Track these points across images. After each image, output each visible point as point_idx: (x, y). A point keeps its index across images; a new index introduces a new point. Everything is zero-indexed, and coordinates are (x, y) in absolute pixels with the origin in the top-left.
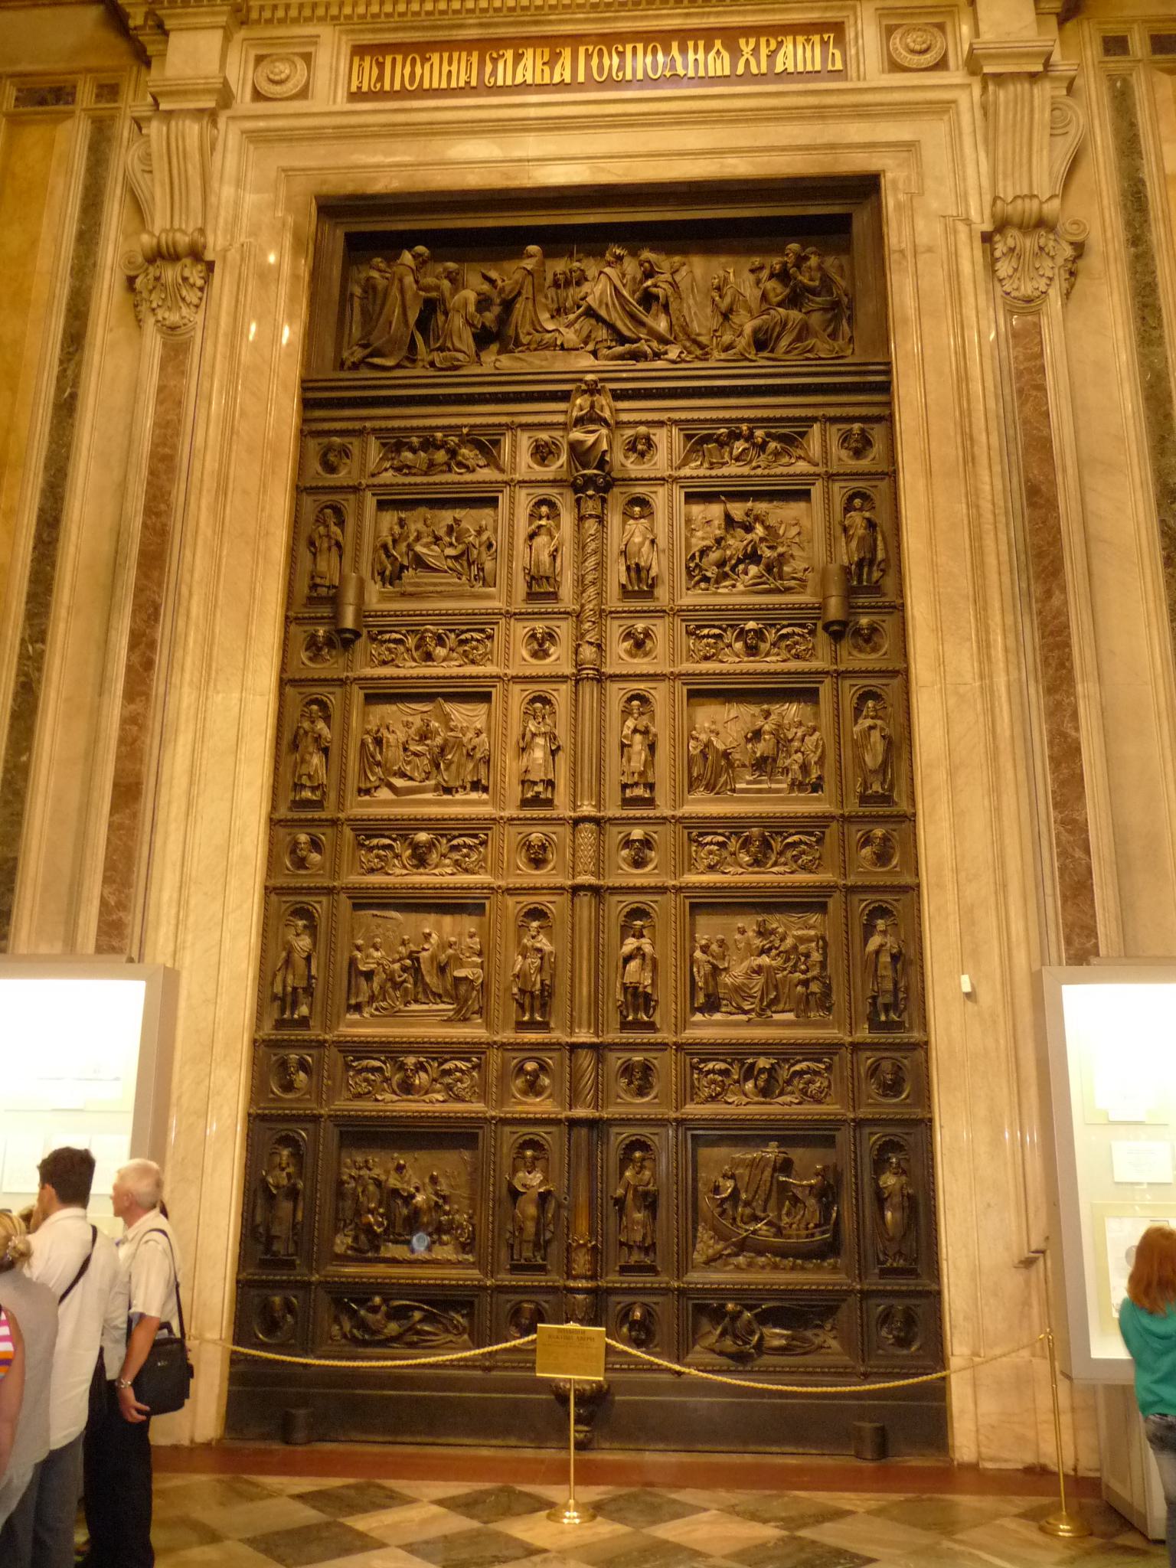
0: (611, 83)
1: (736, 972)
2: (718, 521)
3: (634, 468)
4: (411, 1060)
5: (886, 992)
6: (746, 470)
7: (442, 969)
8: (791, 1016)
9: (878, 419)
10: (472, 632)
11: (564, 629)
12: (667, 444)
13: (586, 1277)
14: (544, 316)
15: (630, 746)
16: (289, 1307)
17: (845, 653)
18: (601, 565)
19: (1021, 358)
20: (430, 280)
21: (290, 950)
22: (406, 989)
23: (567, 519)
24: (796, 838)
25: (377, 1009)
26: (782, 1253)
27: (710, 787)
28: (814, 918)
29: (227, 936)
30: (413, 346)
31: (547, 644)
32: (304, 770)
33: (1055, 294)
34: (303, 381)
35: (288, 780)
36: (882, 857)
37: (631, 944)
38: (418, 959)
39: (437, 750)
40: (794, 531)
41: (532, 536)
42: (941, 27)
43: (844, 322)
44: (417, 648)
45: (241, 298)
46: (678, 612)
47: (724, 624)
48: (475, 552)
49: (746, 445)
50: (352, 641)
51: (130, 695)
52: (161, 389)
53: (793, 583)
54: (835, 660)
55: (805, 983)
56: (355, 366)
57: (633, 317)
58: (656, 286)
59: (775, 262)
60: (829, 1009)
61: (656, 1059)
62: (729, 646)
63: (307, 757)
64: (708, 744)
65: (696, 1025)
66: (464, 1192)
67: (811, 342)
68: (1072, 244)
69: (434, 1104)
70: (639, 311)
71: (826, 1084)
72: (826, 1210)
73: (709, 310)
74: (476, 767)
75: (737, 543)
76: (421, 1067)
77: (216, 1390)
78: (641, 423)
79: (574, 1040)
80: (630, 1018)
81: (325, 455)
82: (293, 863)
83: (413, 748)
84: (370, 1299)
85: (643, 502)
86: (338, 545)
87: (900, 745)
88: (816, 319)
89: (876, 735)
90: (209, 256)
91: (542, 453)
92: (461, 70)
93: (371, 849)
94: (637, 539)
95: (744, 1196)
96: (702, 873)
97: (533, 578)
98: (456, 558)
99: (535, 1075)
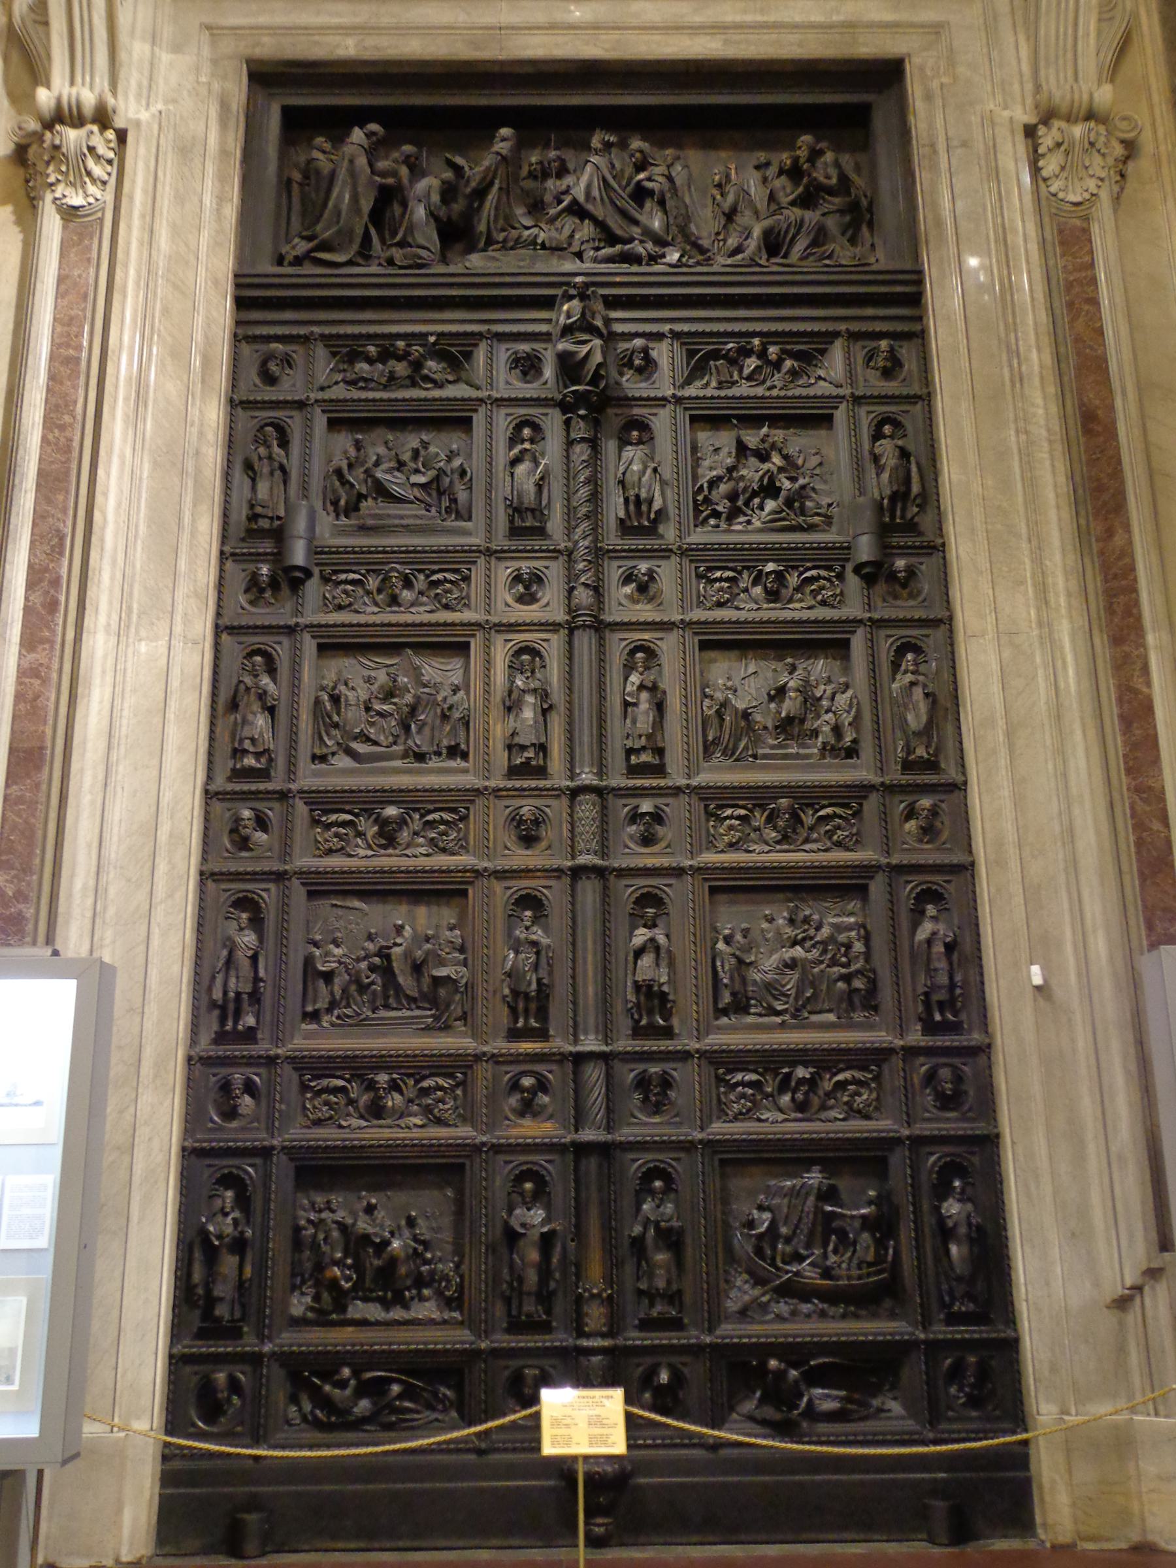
1: (767, 964)
3: (632, 385)
4: (383, 1078)
5: (940, 987)
6: (760, 391)
7: (417, 968)
11: (554, 571)
13: (603, 1336)
14: (520, 211)
15: (635, 705)
16: (234, 1385)
17: (880, 604)
18: (595, 497)
19: (1070, 267)
20: (382, 165)
22: (374, 992)
24: (829, 810)
25: (338, 1017)
26: (832, 1297)
27: (728, 752)
28: (853, 905)
29: (156, 931)
30: (366, 239)
32: (247, 732)
33: (1104, 195)
34: (236, 276)
36: (929, 831)
37: (641, 936)
38: (388, 957)
39: (406, 709)
40: (814, 461)
43: (865, 229)
44: (379, 591)
45: (160, 174)
46: (683, 552)
47: (739, 566)
48: (448, 480)
49: (759, 363)
50: (302, 582)
52: (61, 280)
53: (817, 519)
54: (870, 607)
55: (847, 978)
56: (298, 261)
57: (623, 213)
58: (649, 179)
59: (785, 158)
60: (876, 1008)
61: (677, 1072)
62: (746, 590)
63: (250, 717)
65: (719, 1028)
66: (447, 1236)
67: (830, 247)
68: (1122, 142)
69: (410, 1130)
70: (631, 207)
71: (874, 1095)
72: (880, 1244)
74: (454, 728)
75: (752, 472)
76: (394, 1086)
77: (147, 1494)
78: (637, 335)
79: (579, 1048)
80: (644, 1022)
81: (264, 363)
82: (233, 842)
83: (377, 707)
84: (337, 1372)
85: (643, 426)
86: (282, 469)
88: (831, 223)
89: (918, 692)
90: (119, 123)
93: (328, 826)
94: (635, 467)
95: (784, 1230)
96: (722, 851)
97: (516, 510)
98: (423, 486)
99: (533, 1091)
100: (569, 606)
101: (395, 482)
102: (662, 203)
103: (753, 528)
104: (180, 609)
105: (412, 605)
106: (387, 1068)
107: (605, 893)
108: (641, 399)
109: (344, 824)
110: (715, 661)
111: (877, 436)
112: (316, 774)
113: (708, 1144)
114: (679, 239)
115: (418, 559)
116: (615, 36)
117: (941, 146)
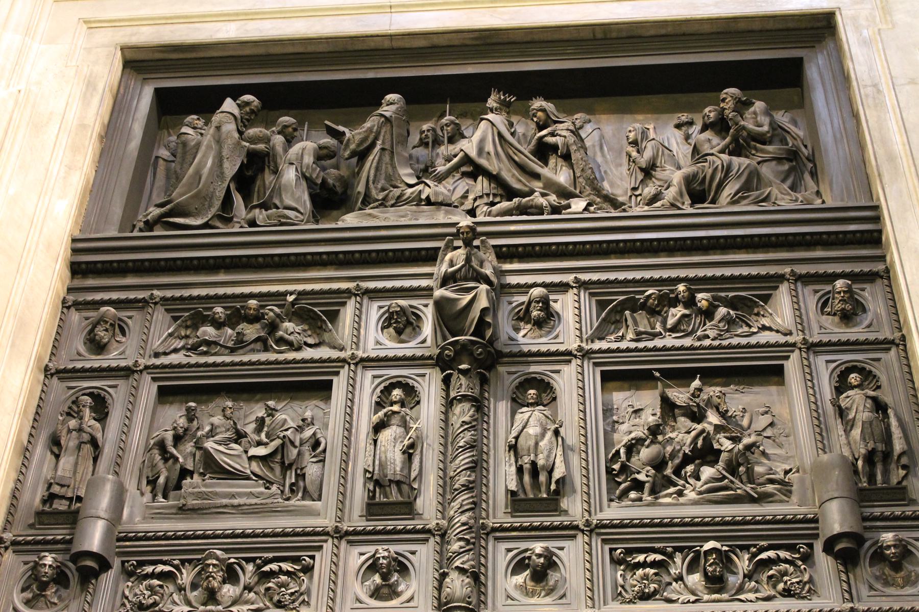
3: (528, 339)
6: (687, 342)
9: (870, 277)
11: (423, 557)
12: (573, 314)
17: (865, 591)
18: (477, 466)
30: (227, 201)
31: (395, 577)
34: (74, 240)
40: (764, 421)
41: (379, 427)
43: (807, 176)
44: (194, 586)
46: (593, 529)
48: (295, 451)
49: (687, 312)
50: (96, 574)
53: (770, 488)
57: (522, 168)
58: (553, 134)
62: (679, 578)
73: (624, 169)
75: (682, 435)
85: (544, 387)
91: (401, 323)
94: (533, 430)
97: (377, 483)
98: (263, 459)
100: (439, 599)
101: (230, 456)
102: (567, 157)
103: (686, 503)
108: (539, 354)
114: (588, 190)
117: (885, 86)
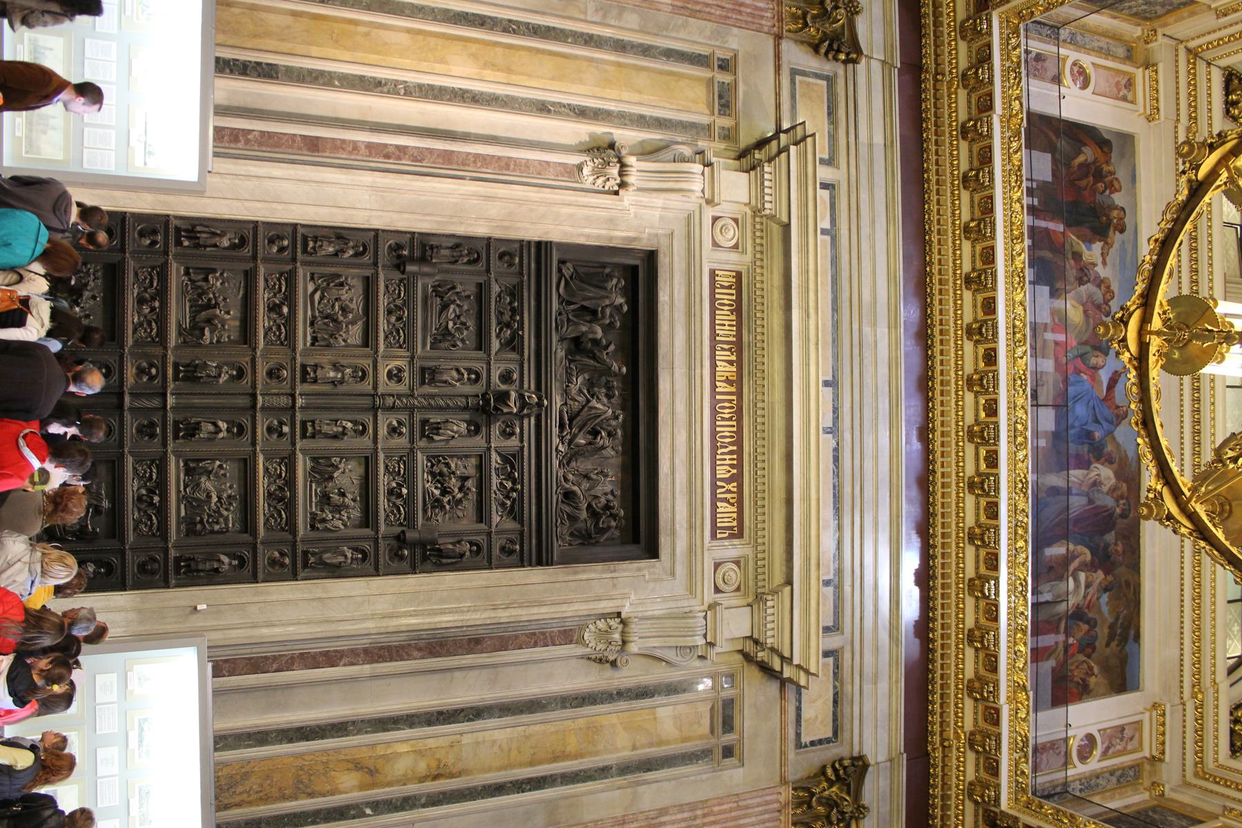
0: (714, 413)
1: (207, 484)
2: (466, 473)
3: (496, 429)
4: (157, 304)
6: (494, 488)
8: (183, 514)
9: (522, 560)
10: (403, 336)
11: (402, 388)
18: (440, 408)
20: (608, 311)
21: (221, 235)
23: (468, 389)
29: (229, 202)
32: (325, 243)
35: (319, 233)
36: (273, 562)
37: (223, 425)
40: (460, 514)
41: (458, 370)
42: (738, 589)
46: (412, 450)
51: (369, 146)
52: (547, 163)
55: (201, 522)
56: (560, 270)
59: (616, 504)
60: (187, 535)
64: (337, 468)
75: (454, 483)
76: (153, 309)
87: (336, 571)
88: (580, 525)
89: (341, 559)
92: (726, 332)
93: (279, 280)
94: (455, 428)
99: (149, 373)
102: (590, 443)
103: (424, 483)
104: (385, 214)
105: (388, 322)
106: (161, 306)
107: (244, 409)
109: (280, 288)
110: (360, 464)
111: (471, 544)
112: (305, 276)
113: (123, 454)
115: (409, 326)
116: (669, 422)
